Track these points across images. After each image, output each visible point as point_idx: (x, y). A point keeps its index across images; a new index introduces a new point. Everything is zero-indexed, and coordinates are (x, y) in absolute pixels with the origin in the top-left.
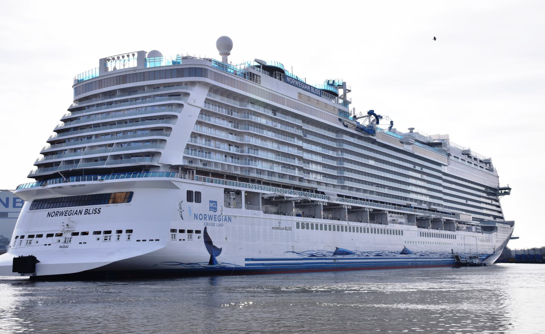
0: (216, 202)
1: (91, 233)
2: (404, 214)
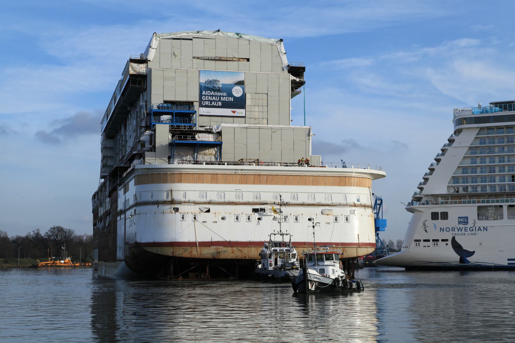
0: (467, 218)
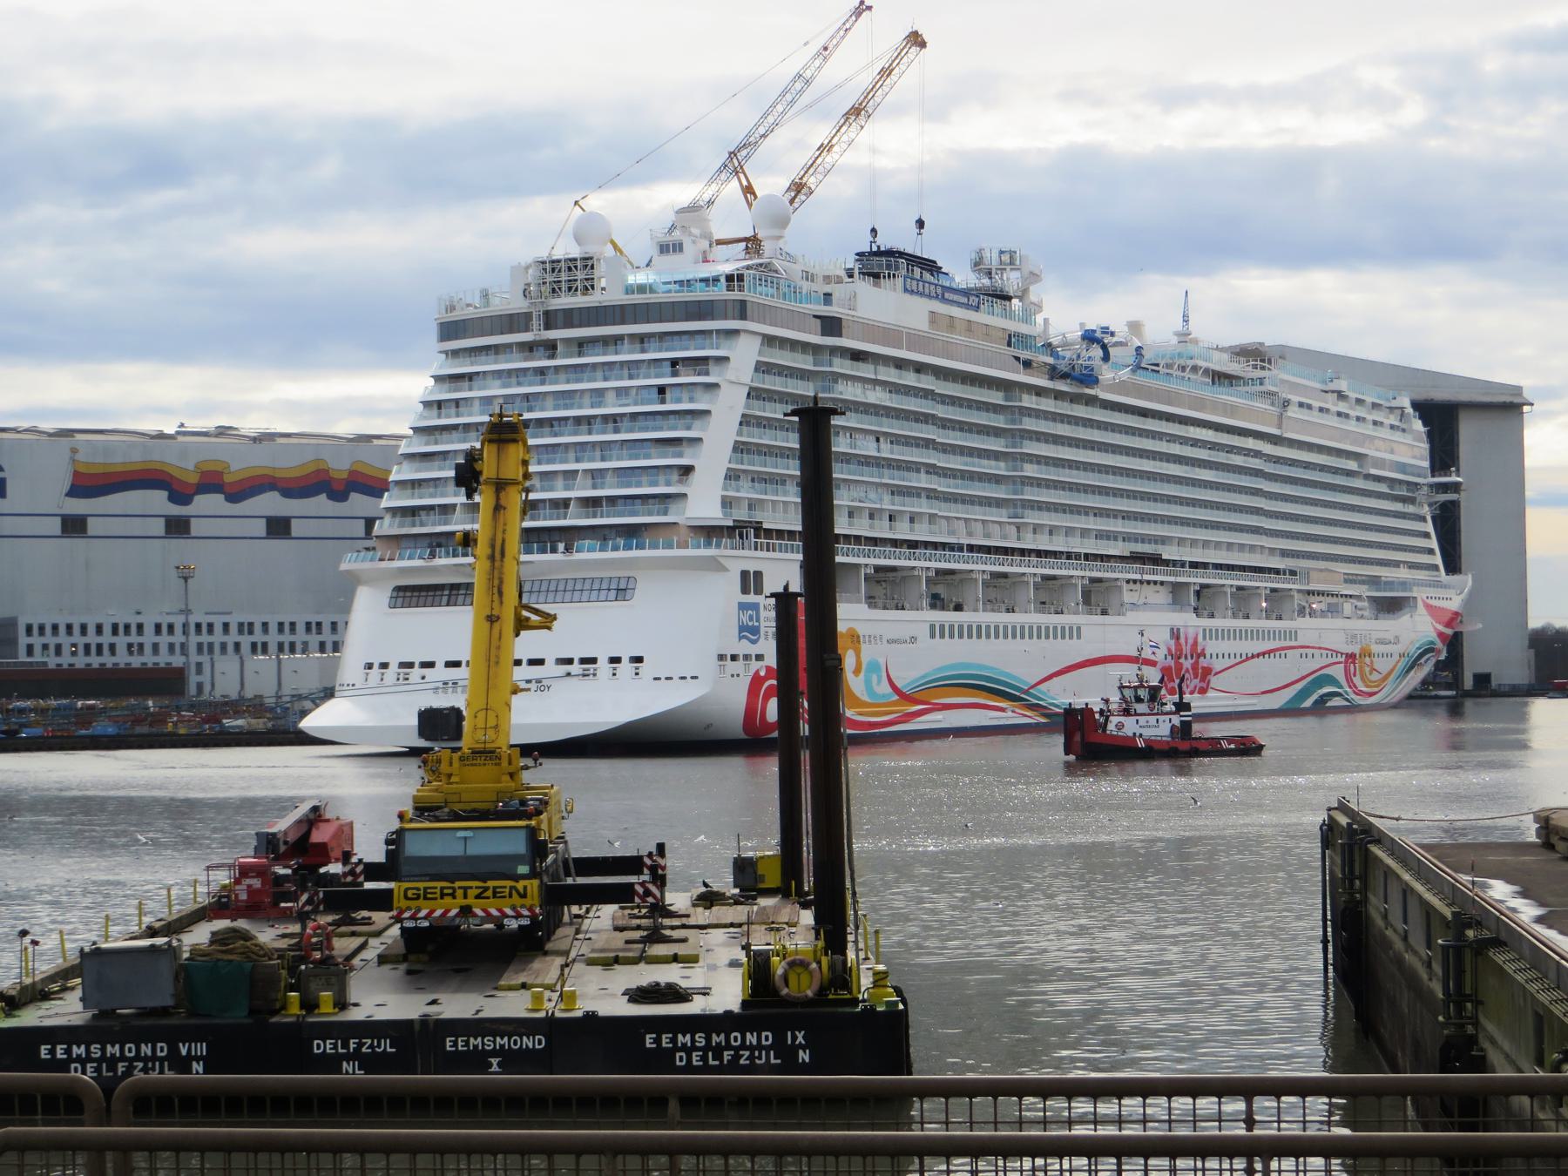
1: (550, 662)
2: (1162, 583)
